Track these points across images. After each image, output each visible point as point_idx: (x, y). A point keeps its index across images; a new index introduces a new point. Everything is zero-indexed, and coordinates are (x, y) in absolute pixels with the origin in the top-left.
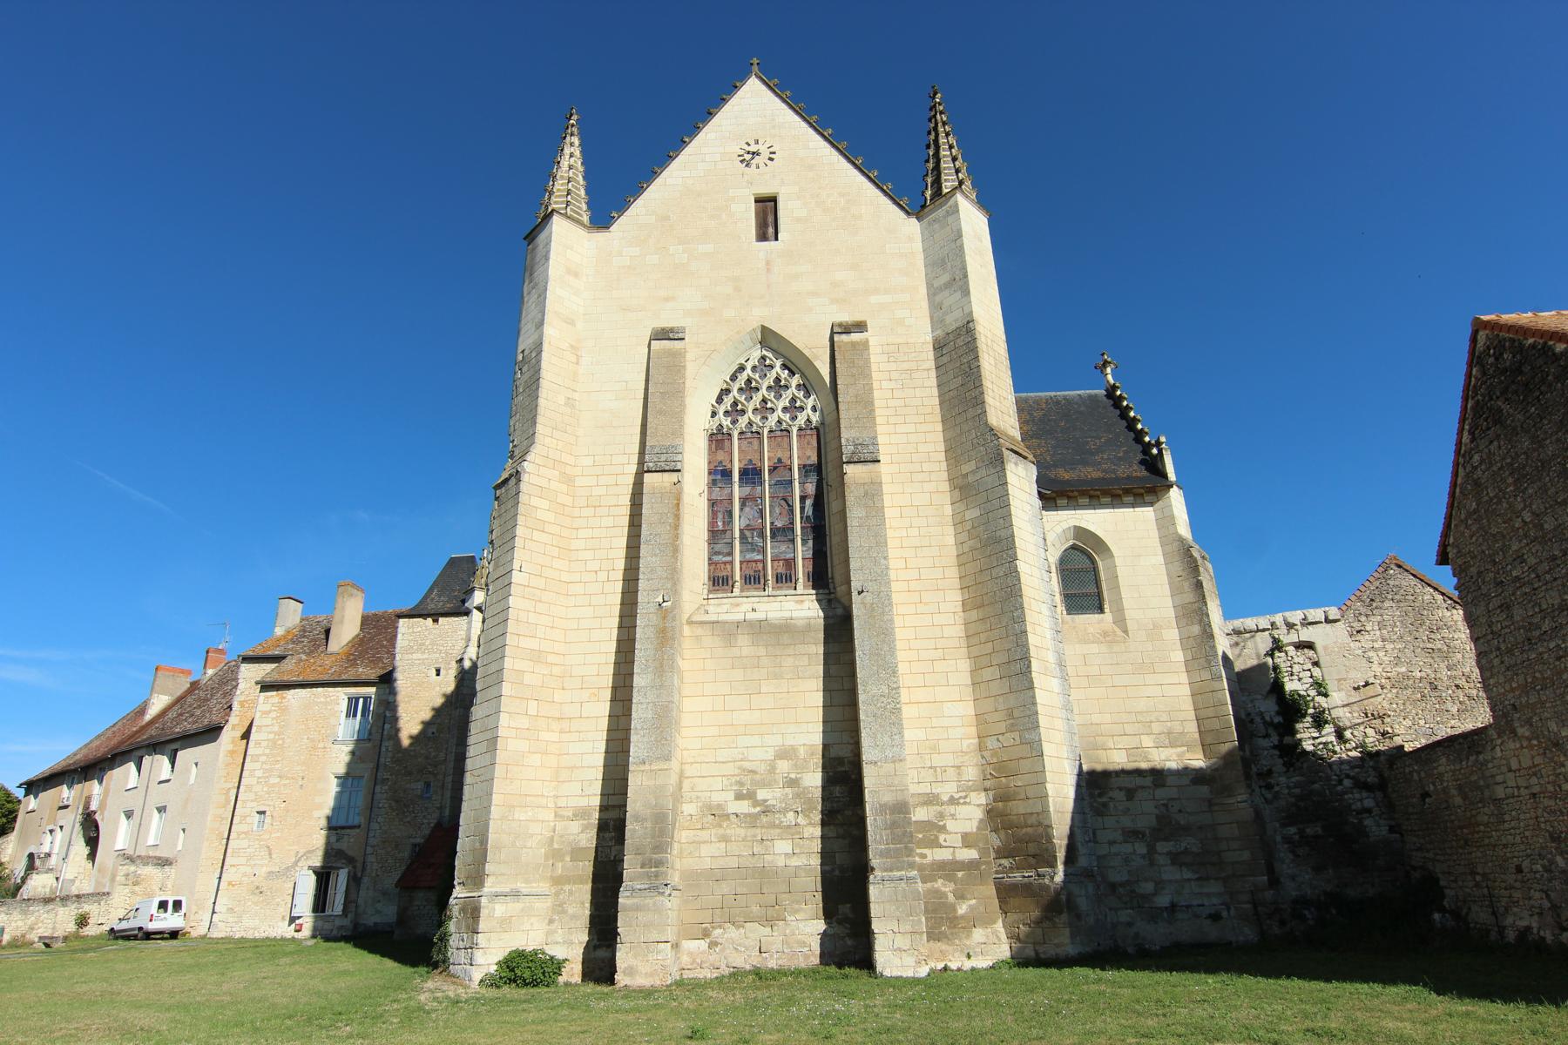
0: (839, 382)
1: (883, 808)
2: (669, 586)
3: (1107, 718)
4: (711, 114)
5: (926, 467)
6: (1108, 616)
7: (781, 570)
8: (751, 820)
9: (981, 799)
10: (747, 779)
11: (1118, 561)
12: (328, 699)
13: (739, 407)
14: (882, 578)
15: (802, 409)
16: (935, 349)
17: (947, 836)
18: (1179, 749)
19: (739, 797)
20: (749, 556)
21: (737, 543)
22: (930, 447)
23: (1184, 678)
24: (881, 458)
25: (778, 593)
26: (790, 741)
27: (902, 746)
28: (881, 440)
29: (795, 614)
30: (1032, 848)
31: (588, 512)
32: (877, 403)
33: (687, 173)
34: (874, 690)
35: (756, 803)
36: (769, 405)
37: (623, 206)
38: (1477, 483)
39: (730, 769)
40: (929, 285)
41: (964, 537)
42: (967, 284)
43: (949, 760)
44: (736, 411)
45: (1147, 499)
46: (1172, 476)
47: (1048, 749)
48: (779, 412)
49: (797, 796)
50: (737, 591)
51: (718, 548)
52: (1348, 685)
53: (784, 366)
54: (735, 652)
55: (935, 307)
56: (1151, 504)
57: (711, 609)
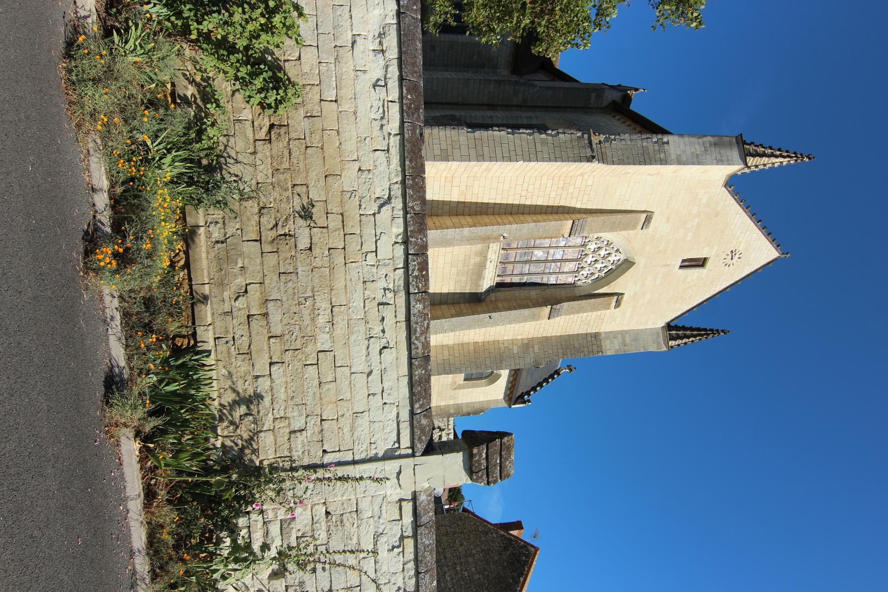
4: (768, 235)
5: (541, 330)
6: (462, 382)
11: (483, 388)
14: (496, 324)
25: (497, 270)
31: (561, 184)
38: (487, 533)
40: (627, 332)
45: (507, 398)
46: (513, 406)
56: (504, 398)
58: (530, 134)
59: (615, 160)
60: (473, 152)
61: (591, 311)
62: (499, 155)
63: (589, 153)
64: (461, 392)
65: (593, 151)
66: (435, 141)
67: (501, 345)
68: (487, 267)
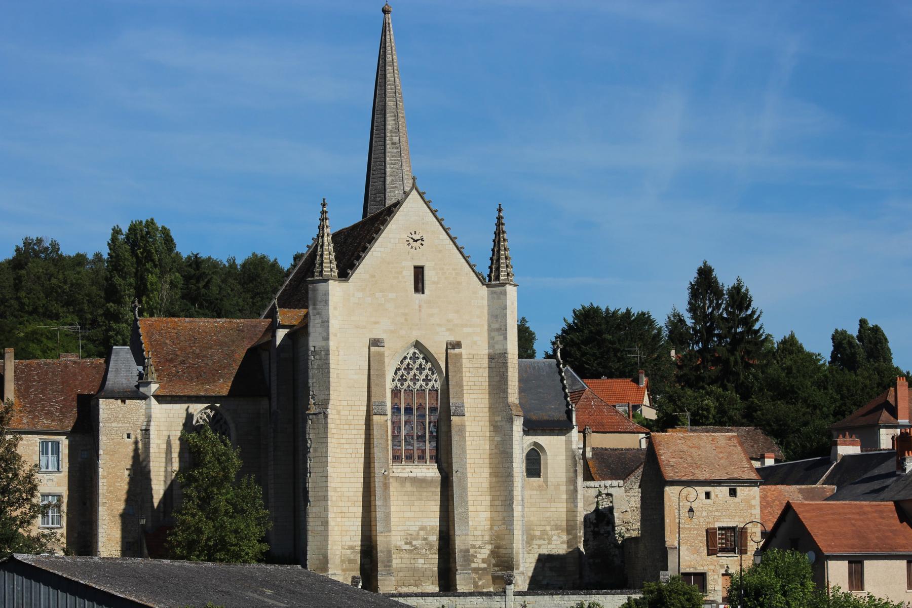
0: (450, 374)
1: (461, 551)
3: (536, 519)
5: (481, 414)
6: (541, 479)
7: (420, 454)
8: (410, 552)
9: (489, 547)
10: (409, 537)
12: (29, 442)
13: (404, 377)
15: (430, 380)
16: (489, 358)
17: (477, 560)
19: (406, 543)
20: (408, 447)
22: (482, 405)
23: (565, 505)
24: (466, 414)
26: (424, 524)
27: (468, 530)
30: (506, 564)
31: (346, 427)
32: (465, 383)
33: (382, 250)
34: (460, 510)
35: (412, 546)
36: (417, 377)
37: (353, 267)
39: (403, 533)
40: (489, 326)
41: (493, 447)
44: (402, 380)
46: (574, 423)
47: (515, 532)
48: (421, 382)
49: (426, 544)
50: (403, 463)
51: (395, 443)
52: (620, 511)
53: (423, 358)
54: (405, 489)
55: (491, 338)
56: (565, 434)
57: (394, 470)
58: (311, 460)
59: (326, 393)
60: (323, 503)
61: (462, 372)
62: (323, 485)
63: (321, 416)
64: (551, 479)
65: (320, 413)
66: (316, 529)
67: (494, 452)
68: (415, 475)
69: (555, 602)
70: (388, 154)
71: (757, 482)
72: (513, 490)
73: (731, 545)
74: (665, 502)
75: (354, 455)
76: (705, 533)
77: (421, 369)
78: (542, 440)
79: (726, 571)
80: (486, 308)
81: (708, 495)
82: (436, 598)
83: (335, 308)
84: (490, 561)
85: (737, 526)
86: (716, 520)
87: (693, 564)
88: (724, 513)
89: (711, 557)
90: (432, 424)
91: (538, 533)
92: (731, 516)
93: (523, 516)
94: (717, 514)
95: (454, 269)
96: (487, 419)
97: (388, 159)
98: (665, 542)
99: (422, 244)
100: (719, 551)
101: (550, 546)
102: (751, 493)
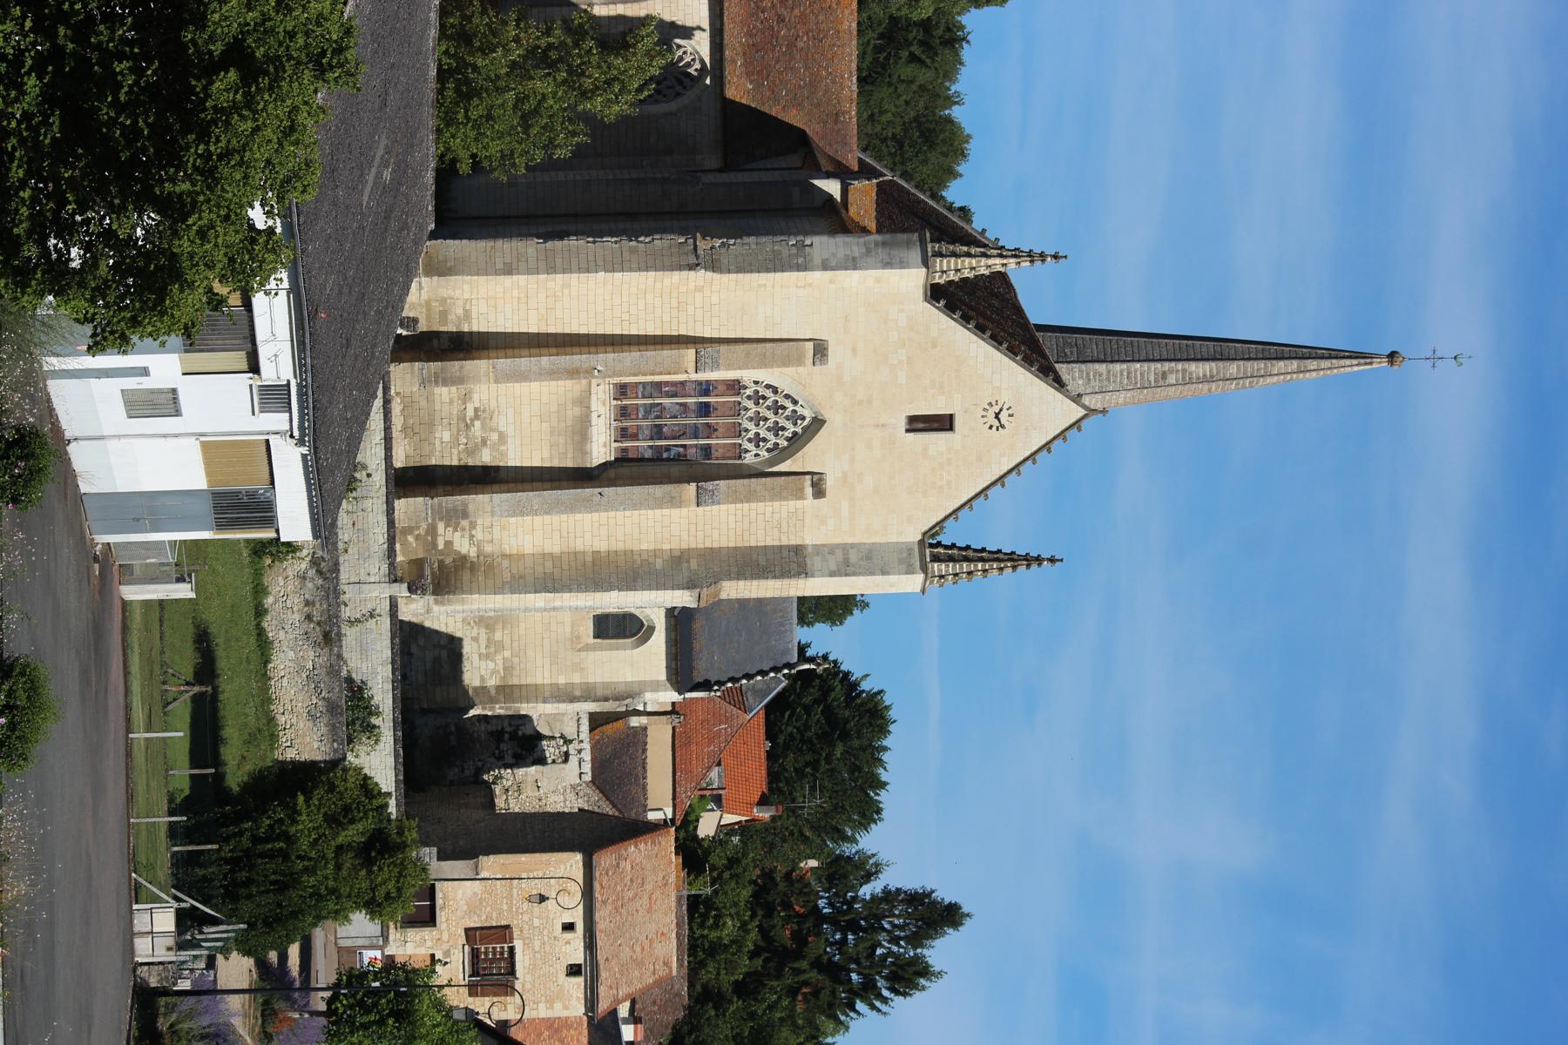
0: (768, 479)
1: (465, 505)
2: (609, 373)
6: (591, 640)
7: (630, 431)
8: (462, 418)
9: (473, 553)
10: (487, 415)
13: (761, 401)
14: (611, 507)
15: (757, 446)
16: (797, 546)
18: (502, 671)
19: (476, 410)
20: (641, 409)
21: (650, 401)
23: (547, 681)
24: (700, 508)
25: (612, 431)
28: (723, 507)
29: (594, 445)
30: (443, 582)
31: (674, 303)
32: (753, 505)
35: (472, 420)
36: (762, 423)
37: (950, 309)
39: (493, 404)
40: (853, 546)
41: (645, 556)
42: (840, 575)
43: (496, 536)
44: (757, 398)
46: (689, 695)
47: (499, 597)
48: (753, 429)
49: (476, 445)
50: (615, 402)
51: (648, 388)
52: (539, 777)
53: (795, 434)
55: (832, 549)
56: (669, 679)
57: (601, 387)
58: (616, 242)
59: (732, 267)
60: (542, 265)
61: (772, 499)
62: (575, 266)
63: (693, 260)
65: (697, 258)
66: (497, 254)
67: (636, 557)
69: (380, 668)
70: (1146, 365)
71: (593, 1012)
72: (571, 592)
73: (485, 969)
74: (555, 854)
75: (625, 316)
76: (504, 923)
77: (777, 429)
78: (658, 641)
79: (439, 960)
80: (883, 540)
81: (569, 927)
82: (383, 462)
83: (878, 280)
84: (448, 555)
85: (517, 979)
86: (527, 942)
87: (451, 903)
88: (538, 956)
89: (463, 934)
90: (681, 450)
91: (498, 636)
92: (533, 968)
93: (526, 610)
94: (537, 944)
95: (949, 482)
96: (693, 546)
97: (1138, 365)
98: (487, 854)
99: (991, 427)
100: (473, 949)
101: (476, 657)
102: (574, 1002)
